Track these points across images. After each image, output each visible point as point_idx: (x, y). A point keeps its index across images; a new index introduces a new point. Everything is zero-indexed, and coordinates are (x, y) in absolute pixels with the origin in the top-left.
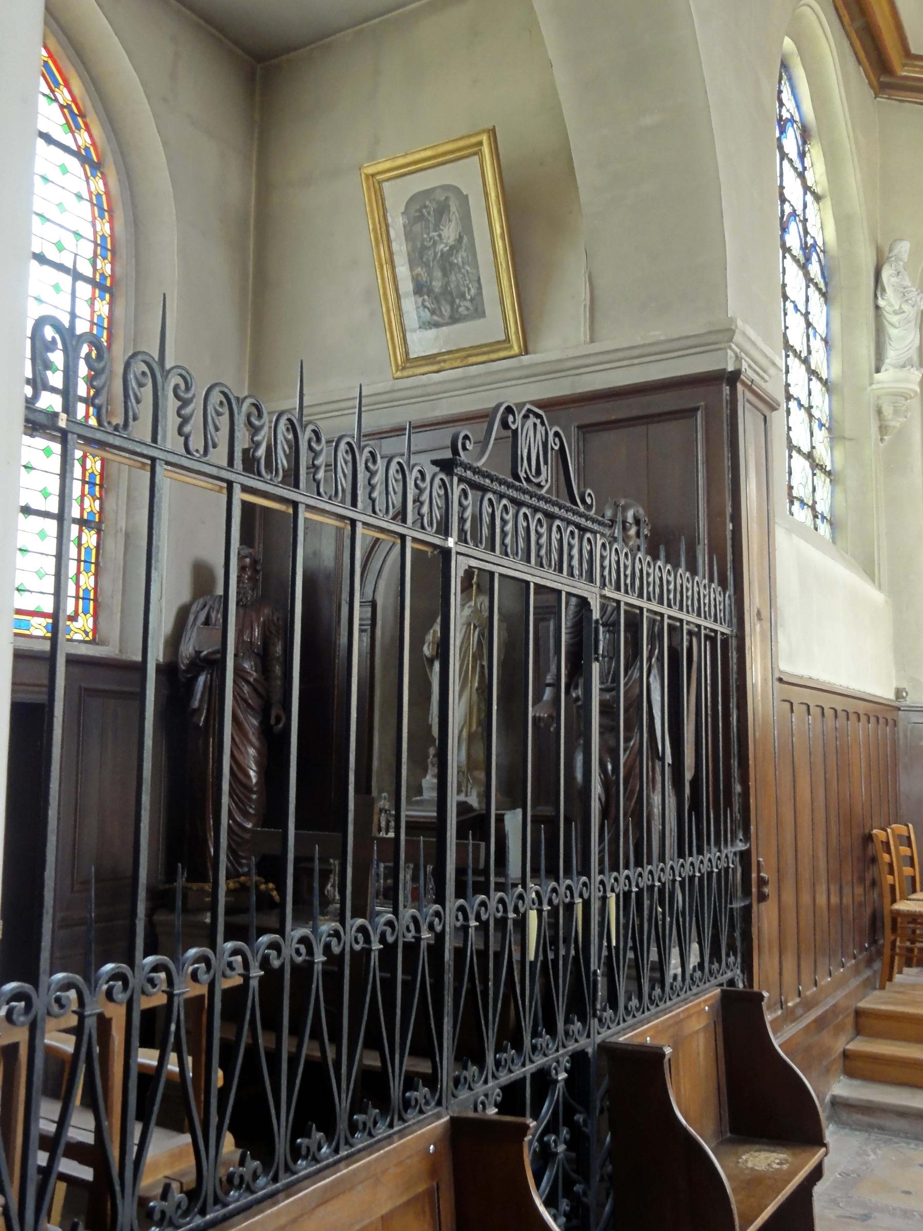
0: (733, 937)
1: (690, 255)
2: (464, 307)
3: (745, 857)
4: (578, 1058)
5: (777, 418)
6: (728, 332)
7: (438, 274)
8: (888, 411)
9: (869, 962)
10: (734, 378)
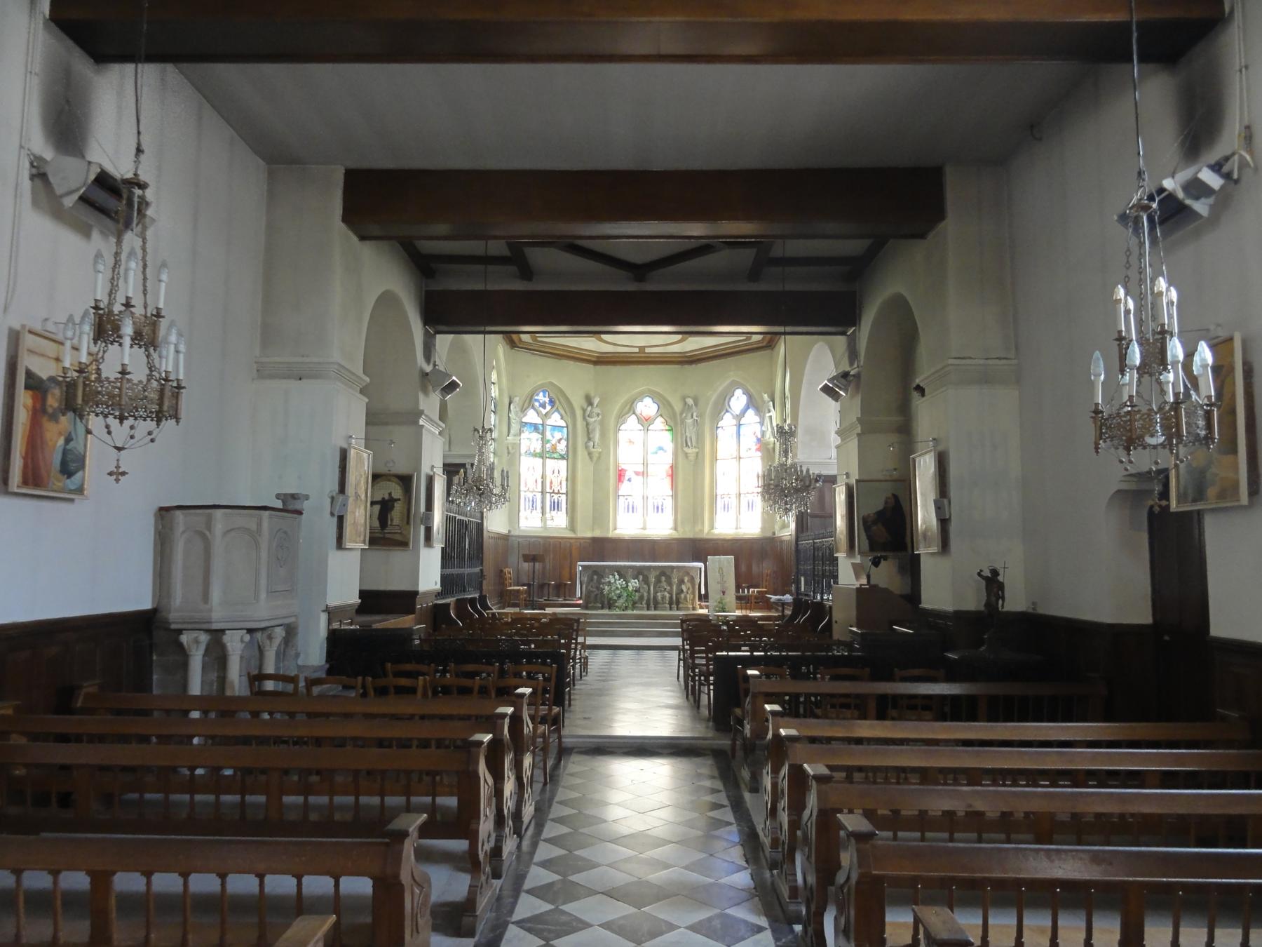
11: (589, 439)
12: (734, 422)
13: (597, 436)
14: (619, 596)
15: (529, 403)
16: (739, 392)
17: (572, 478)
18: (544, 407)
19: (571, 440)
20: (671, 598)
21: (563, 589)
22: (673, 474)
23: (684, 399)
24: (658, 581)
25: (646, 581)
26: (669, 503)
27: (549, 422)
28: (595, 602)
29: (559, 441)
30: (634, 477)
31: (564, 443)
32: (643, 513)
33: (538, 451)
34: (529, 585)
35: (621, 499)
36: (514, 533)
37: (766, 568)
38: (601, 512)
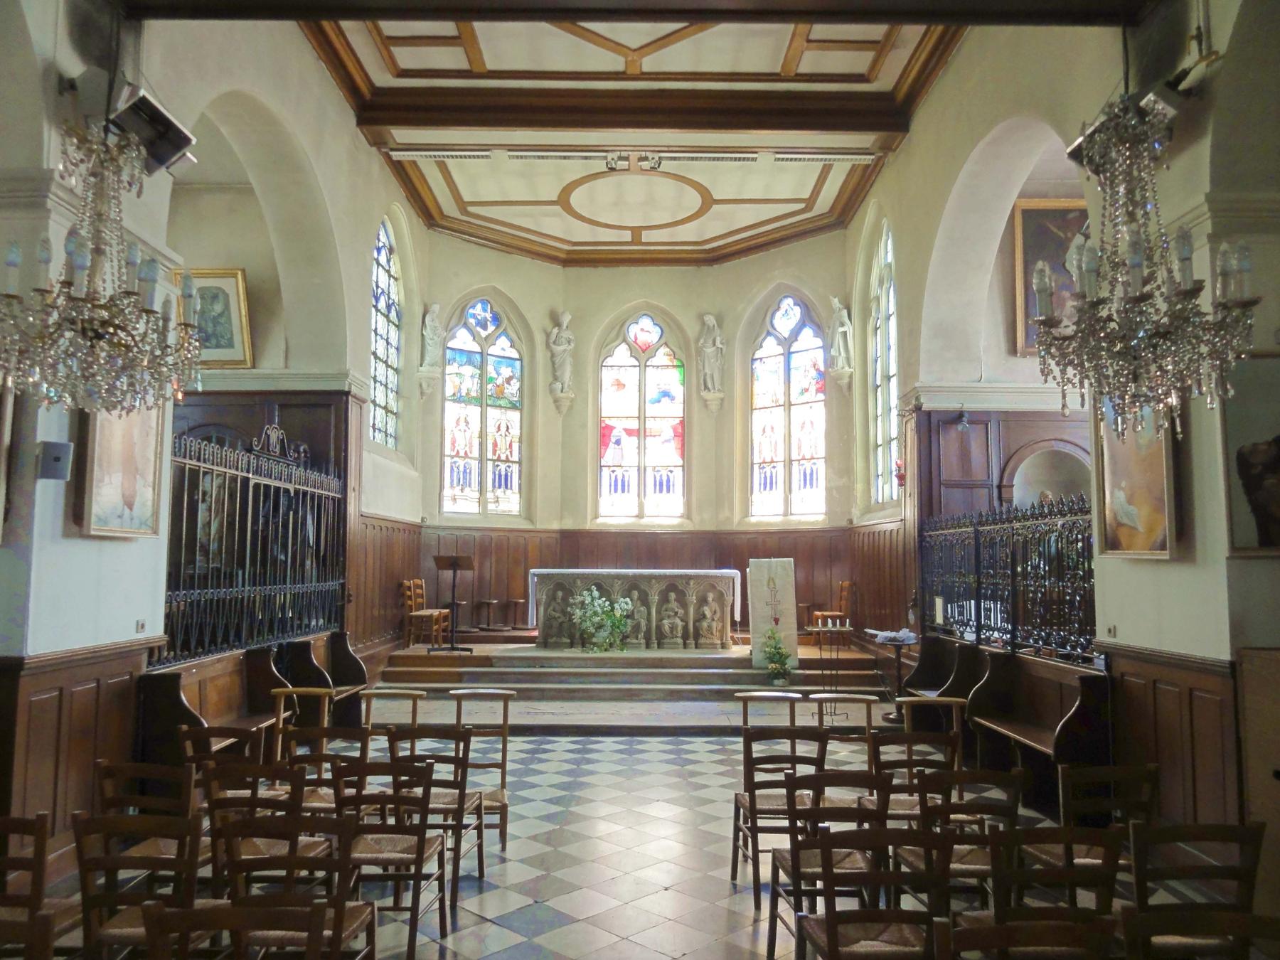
0: (335, 608)
1: (330, 328)
2: (223, 342)
3: (343, 585)
4: (280, 646)
5: (365, 406)
6: (346, 375)
7: (211, 325)
8: (424, 385)
9: (398, 639)
10: (347, 394)
11: (556, 378)
12: (780, 350)
13: (567, 374)
14: (600, 627)
15: (459, 316)
16: (788, 302)
17: (528, 438)
18: (485, 328)
19: (527, 379)
20: (685, 628)
21: (512, 612)
22: (683, 433)
23: (701, 317)
24: (664, 599)
25: (644, 600)
26: (678, 477)
27: (492, 350)
28: (560, 635)
29: (508, 380)
30: (625, 439)
31: (515, 385)
32: (641, 495)
33: (473, 394)
34: (452, 606)
35: (606, 472)
36: (436, 522)
37: (838, 579)
38: (576, 486)
